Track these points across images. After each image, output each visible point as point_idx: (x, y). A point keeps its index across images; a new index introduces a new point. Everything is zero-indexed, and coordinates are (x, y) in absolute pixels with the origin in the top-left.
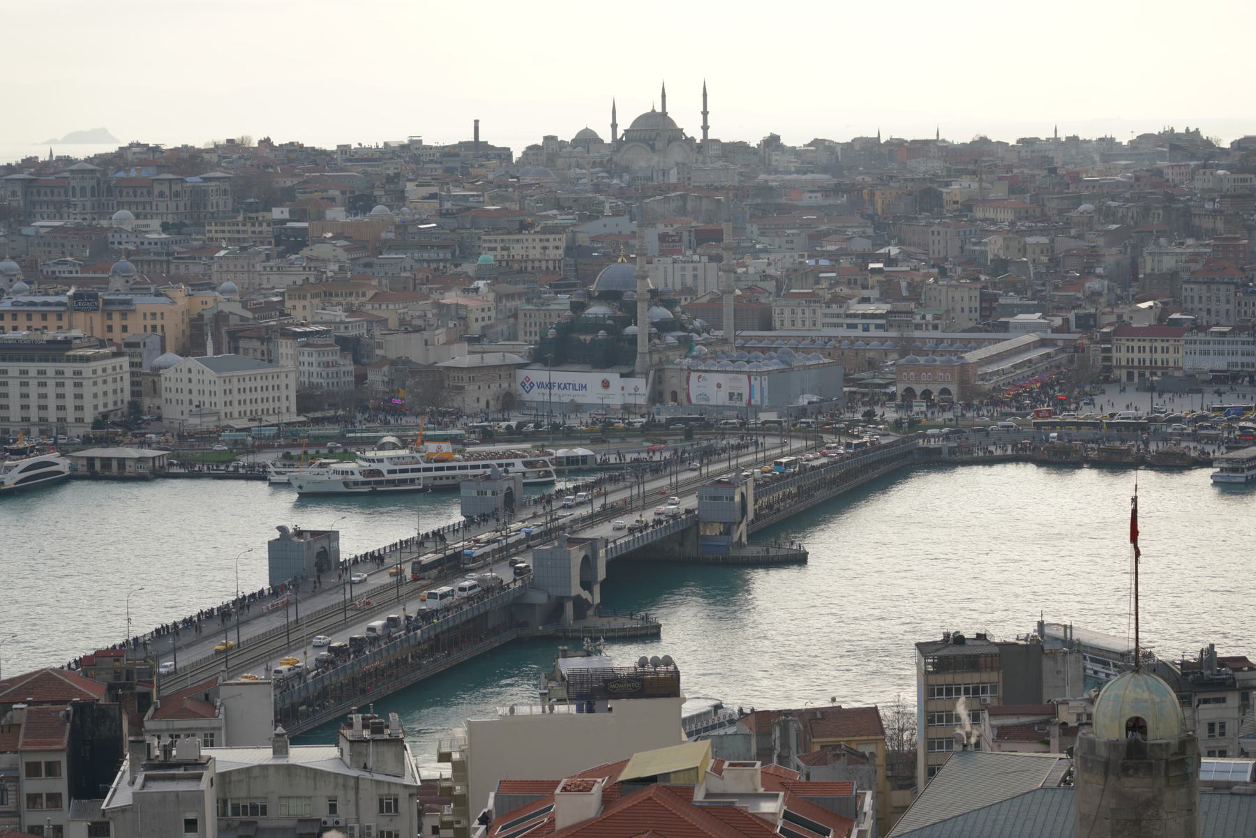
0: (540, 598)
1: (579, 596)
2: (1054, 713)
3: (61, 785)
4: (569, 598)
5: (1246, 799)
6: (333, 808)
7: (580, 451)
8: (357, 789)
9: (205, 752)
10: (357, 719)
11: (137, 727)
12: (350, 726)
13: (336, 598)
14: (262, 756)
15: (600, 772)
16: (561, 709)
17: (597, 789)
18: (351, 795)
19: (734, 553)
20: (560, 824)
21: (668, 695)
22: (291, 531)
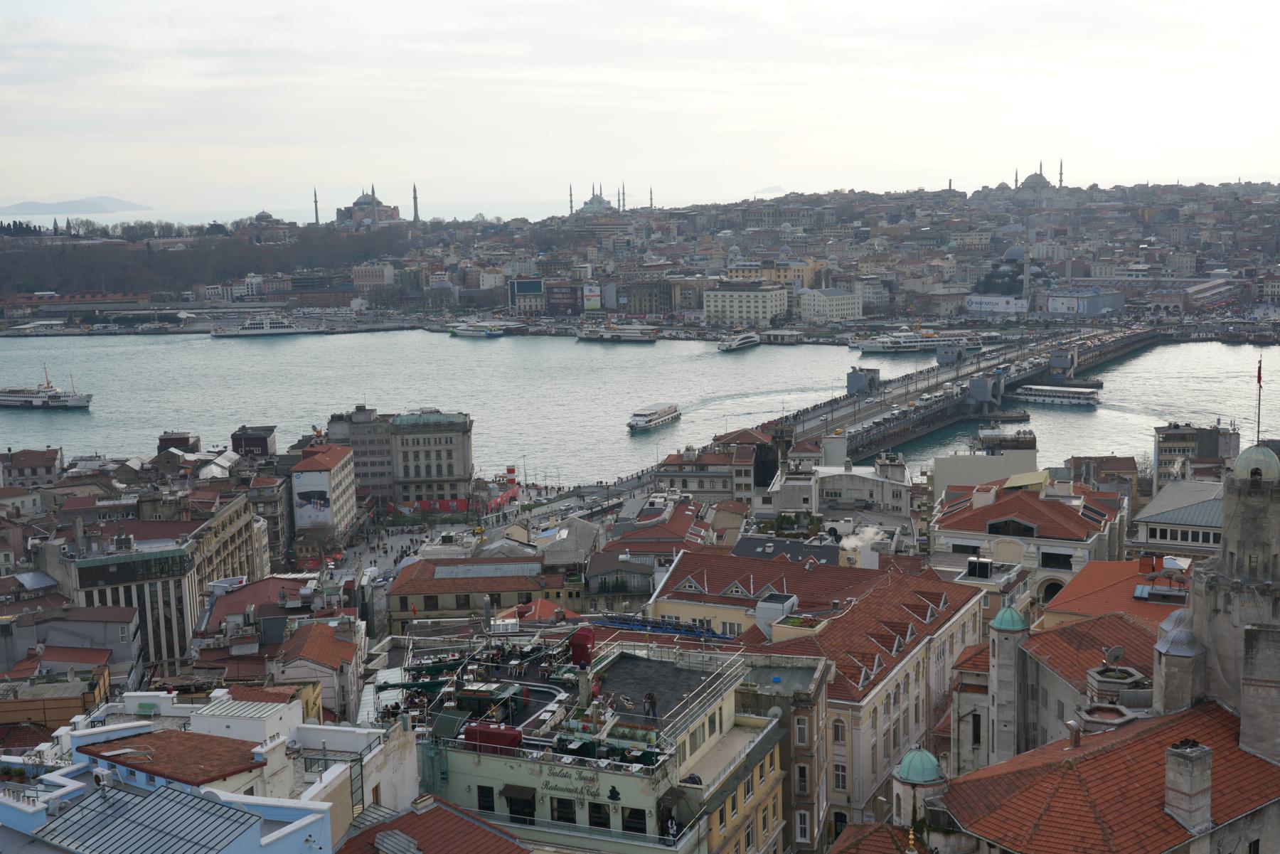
3: (751, 480)
6: (871, 495)
9: (814, 468)
10: (883, 455)
11: (785, 456)
12: (880, 458)
14: (840, 470)
15: (994, 483)
16: (979, 453)
17: (993, 492)
18: (880, 489)
20: (975, 507)
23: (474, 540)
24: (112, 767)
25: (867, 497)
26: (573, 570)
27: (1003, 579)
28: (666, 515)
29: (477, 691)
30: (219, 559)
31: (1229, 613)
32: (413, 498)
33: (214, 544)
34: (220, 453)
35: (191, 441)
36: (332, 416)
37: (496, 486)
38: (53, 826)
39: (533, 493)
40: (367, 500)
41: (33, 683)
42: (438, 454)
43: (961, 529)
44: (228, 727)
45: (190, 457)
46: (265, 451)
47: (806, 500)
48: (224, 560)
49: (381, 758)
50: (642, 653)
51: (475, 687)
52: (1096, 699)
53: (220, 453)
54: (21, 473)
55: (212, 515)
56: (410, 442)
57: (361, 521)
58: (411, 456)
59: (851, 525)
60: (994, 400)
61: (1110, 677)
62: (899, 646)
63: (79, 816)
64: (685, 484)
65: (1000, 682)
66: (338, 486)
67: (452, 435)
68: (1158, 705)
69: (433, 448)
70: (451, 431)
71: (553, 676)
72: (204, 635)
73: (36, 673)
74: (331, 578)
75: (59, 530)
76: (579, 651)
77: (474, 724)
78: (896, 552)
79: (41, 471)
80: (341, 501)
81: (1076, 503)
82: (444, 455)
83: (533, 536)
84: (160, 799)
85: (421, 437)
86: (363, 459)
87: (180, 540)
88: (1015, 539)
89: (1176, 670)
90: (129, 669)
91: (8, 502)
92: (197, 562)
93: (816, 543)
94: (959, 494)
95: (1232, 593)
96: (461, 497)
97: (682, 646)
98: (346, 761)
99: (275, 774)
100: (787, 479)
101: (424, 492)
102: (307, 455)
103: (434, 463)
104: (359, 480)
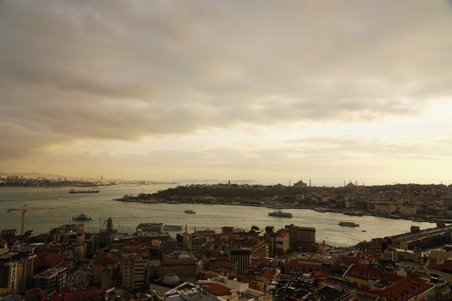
0: (447, 237)
3: (381, 250)
4: (451, 238)
6: (412, 258)
8: (415, 256)
9: (396, 249)
10: (415, 248)
13: (419, 234)
14: (403, 250)
16: (444, 251)
17: (443, 261)
18: (414, 257)
20: (438, 264)
23: (309, 256)
24: (204, 289)
25: (411, 258)
26: (330, 266)
28: (354, 256)
29: (290, 289)
30: (258, 253)
32: (302, 245)
33: (257, 249)
34: (263, 231)
35: (258, 228)
36: (286, 226)
37: (320, 245)
38: (189, 298)
39: (329, 247)
40: (292, 244)
41: (215, 272)
42: (308, 236)
43: (432, 269)
44: (233, 286)
45: (257, 231)
46: (272, 232)
47: (391, 257)
48: (259, 253)
49: (263, 299)
50: (331, 287)
51: (290, 288)
53: (263, 231)
54: (226, 231)
55: (257, 243)
56: (302, 233)
57: (290, 249)
58: (302, 236)
59: (403, 264)
62: (406, 297)
63: (194, 297)
64: (364, 249)
66: (285, 241)
67: (311, 232)
69: (307, 235)
70: (311, 231)
71: (309, 289)
72: (250, 268)
73: (218, 270)
74: (276, 260)
75: (229, 243)
76: (316, 284)
77: (287, 296)
78: (415, 273)
79: (230, 231)
80: (286, 244)
82: (309, 236)
83: (323, 257)
84: (208, 297)
85: (304, 232)
86: (291, 235)
87: (250, 248)
90: (235, 273)
91: (223, 236)
92: (253, 253)
93: (389, 267)
94: (433, 260)
96: (312, 246)
97: (341, 286)
98: (254, 298)
99: (234, 297)
100: (386, 251)
101: (304, 244)
102: (279, 233)
103: (307, 238)
104: (290, 240)
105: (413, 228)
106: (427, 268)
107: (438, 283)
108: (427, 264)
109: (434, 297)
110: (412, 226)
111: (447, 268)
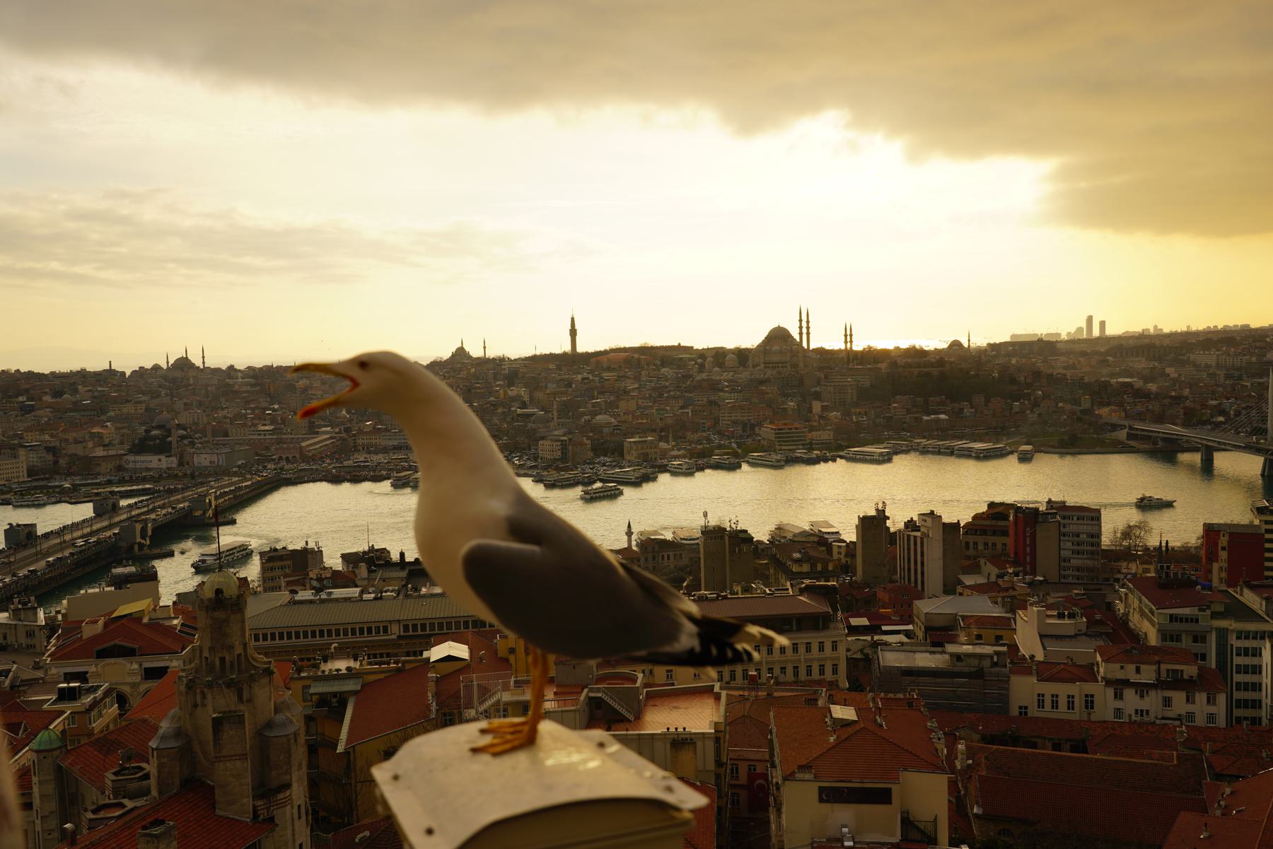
0: (124, 544)
1: (140, 542)
2: (308, 575)
4: (136, 543)
5: (356, 603)
6: (5, 638)
7: (147, 486)
8: (16, 629)
15: (104, 616)
17: (101, 623)
18: (13, 631)
19: (206, 521)
20: (84, 637)
21: (153, 580)
22: (15, 525)
27: (88, 699)
31: (205, 705)
52: (111, 796)
60: (143, 541)
61: (124, 775)
65: (42, 796)
68: (154, 793)
78: (12, 687)
81: (175, 622)
88: (120, 660)
89: (166, 760)
94: (72, 627)
95: (206, 690)
105: (12, 532)
106: (49, 659)
107: (80, 697)
108: (53, 646)
109: (54, 746)
110: (9, 524)
111: (112, 643)
